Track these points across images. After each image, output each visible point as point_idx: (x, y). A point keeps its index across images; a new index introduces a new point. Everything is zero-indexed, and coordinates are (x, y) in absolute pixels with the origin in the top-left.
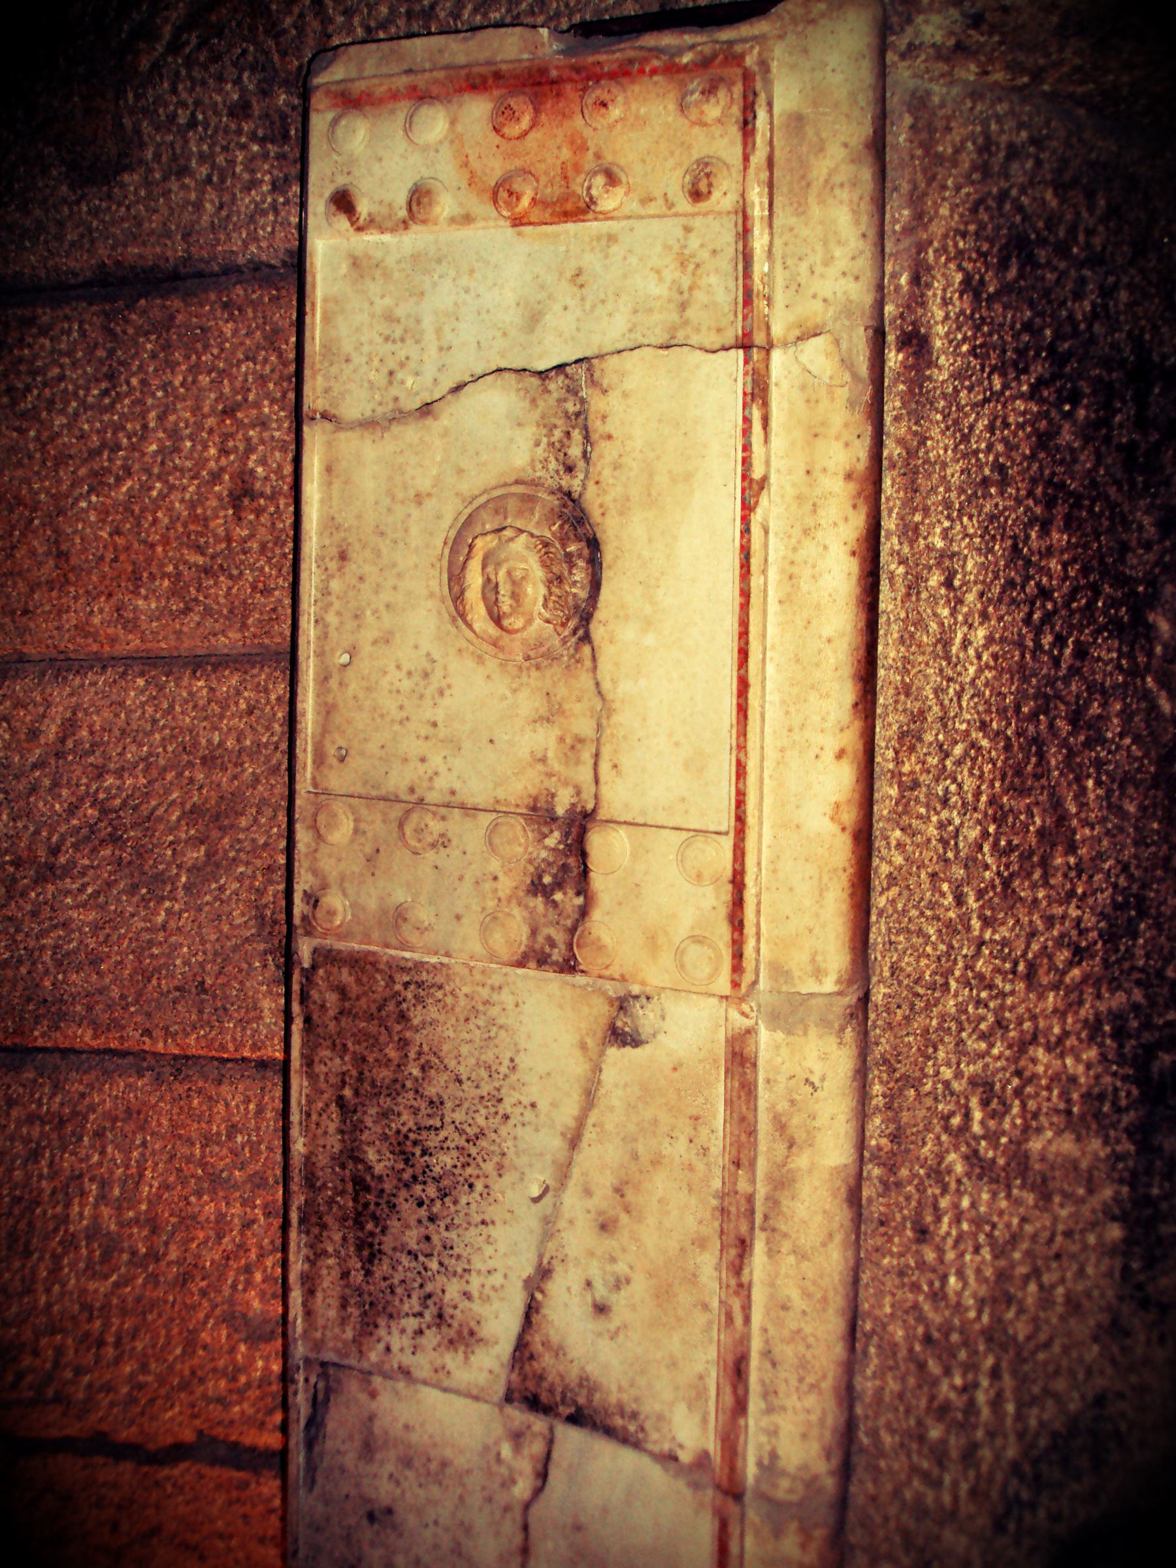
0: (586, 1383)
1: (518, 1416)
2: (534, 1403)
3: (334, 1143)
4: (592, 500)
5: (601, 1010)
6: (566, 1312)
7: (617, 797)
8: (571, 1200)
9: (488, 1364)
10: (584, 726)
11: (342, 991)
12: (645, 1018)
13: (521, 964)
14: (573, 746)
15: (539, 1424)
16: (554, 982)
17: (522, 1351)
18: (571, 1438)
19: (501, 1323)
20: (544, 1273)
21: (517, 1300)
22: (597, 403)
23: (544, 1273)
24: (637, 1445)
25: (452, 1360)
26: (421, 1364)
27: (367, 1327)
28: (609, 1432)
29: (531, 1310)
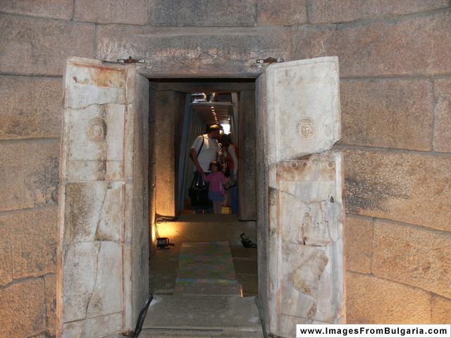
0: (105, 234)
1: (97, 242)
2: (98, 240)
3: (69, 210)
4: (106, 121)
5: (106, 185)
6: (102, 226)
7: (109, 158)
8: (103, 210)
9: (92, 236)
10: (105, 149)
11: (71, 188)
12: (112, 185)
13: (98, 180)
14: (104, 152)
15: (99, 242)
16: (101, 182)
17: (97, 232)
18: (103, 242)
19: (93, 230)
20: (100, 221)
21: (96, 226)
22: (107, 109)
23: (100, 221)
24: (111, 240)
25: (87, 238)
26: (82, 240)
27: (74, 236)
28: (108, 240)
29: (98, 226)
